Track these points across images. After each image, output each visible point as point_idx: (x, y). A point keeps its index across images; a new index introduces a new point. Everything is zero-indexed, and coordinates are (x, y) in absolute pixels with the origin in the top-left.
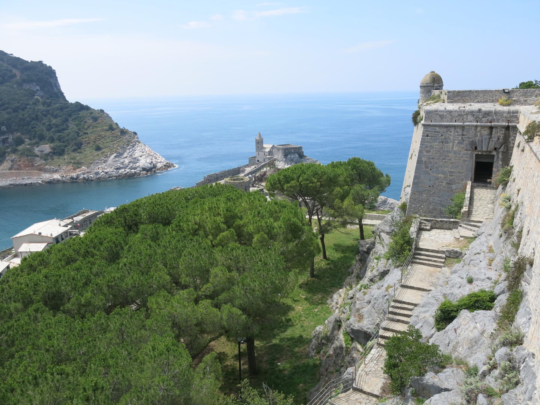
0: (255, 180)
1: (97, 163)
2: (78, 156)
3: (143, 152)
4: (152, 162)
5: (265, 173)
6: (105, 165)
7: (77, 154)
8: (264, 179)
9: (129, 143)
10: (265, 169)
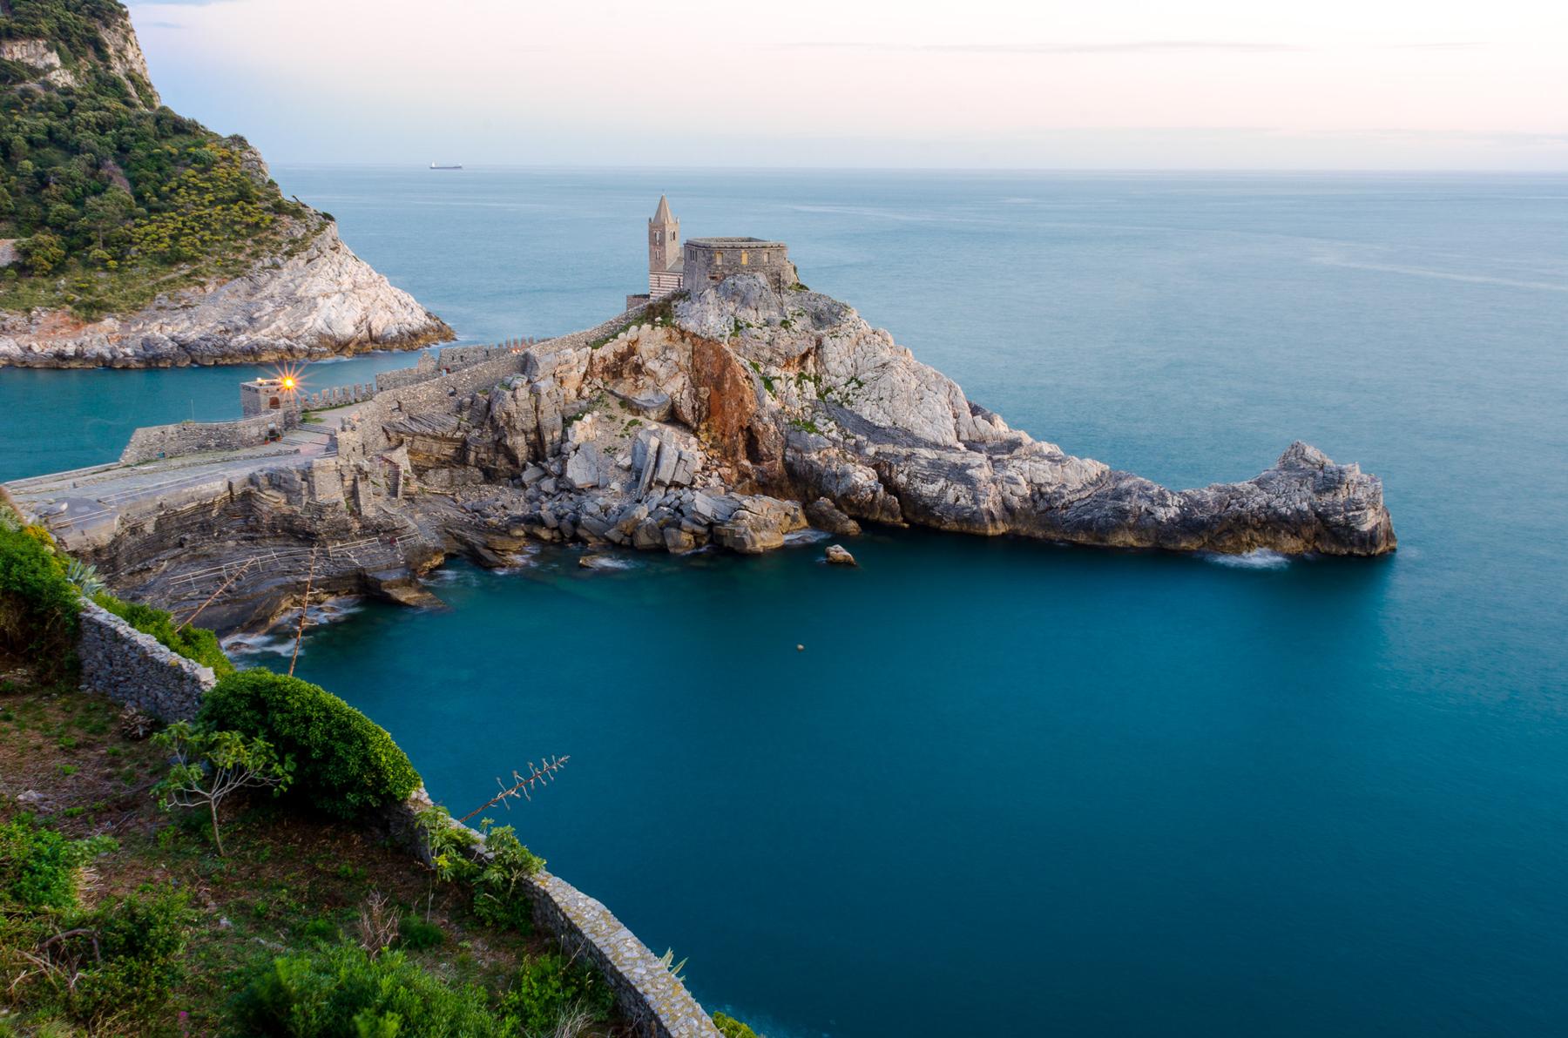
1: (160, 308)
2: (103, 282)
6: (184, 316)
7: (103, 275)
8: (626, 372)
9: (297, 246)
10: (634, 328)
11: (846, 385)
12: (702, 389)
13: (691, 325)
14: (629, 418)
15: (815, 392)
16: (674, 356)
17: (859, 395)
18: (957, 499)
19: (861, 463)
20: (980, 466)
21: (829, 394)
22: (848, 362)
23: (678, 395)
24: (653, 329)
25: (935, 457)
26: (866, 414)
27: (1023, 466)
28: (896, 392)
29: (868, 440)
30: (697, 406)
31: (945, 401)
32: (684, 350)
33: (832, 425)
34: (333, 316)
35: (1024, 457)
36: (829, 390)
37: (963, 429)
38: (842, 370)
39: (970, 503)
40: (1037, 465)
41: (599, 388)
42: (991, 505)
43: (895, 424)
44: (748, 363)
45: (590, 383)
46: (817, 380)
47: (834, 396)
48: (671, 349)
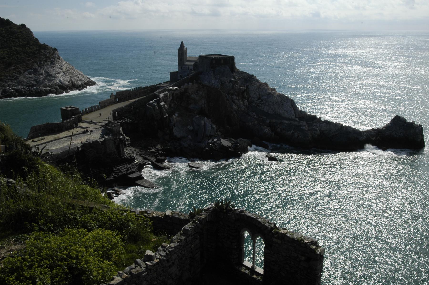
0: (173, 99)
3: (61, 69)
4: (71, 80)
5: (186, 90)
10: (186, 84)
11: (257, 101)
18: (298, 136)
20: (305, 126)
21: (252, 104)
23: (203, 106)
24: (193, 84)
25: (289, 123)
26: (265, 109)
34: (62, 79)
38: (255, 96)
40: (322, 125)
42: (309, 137)
46: (248, 99)
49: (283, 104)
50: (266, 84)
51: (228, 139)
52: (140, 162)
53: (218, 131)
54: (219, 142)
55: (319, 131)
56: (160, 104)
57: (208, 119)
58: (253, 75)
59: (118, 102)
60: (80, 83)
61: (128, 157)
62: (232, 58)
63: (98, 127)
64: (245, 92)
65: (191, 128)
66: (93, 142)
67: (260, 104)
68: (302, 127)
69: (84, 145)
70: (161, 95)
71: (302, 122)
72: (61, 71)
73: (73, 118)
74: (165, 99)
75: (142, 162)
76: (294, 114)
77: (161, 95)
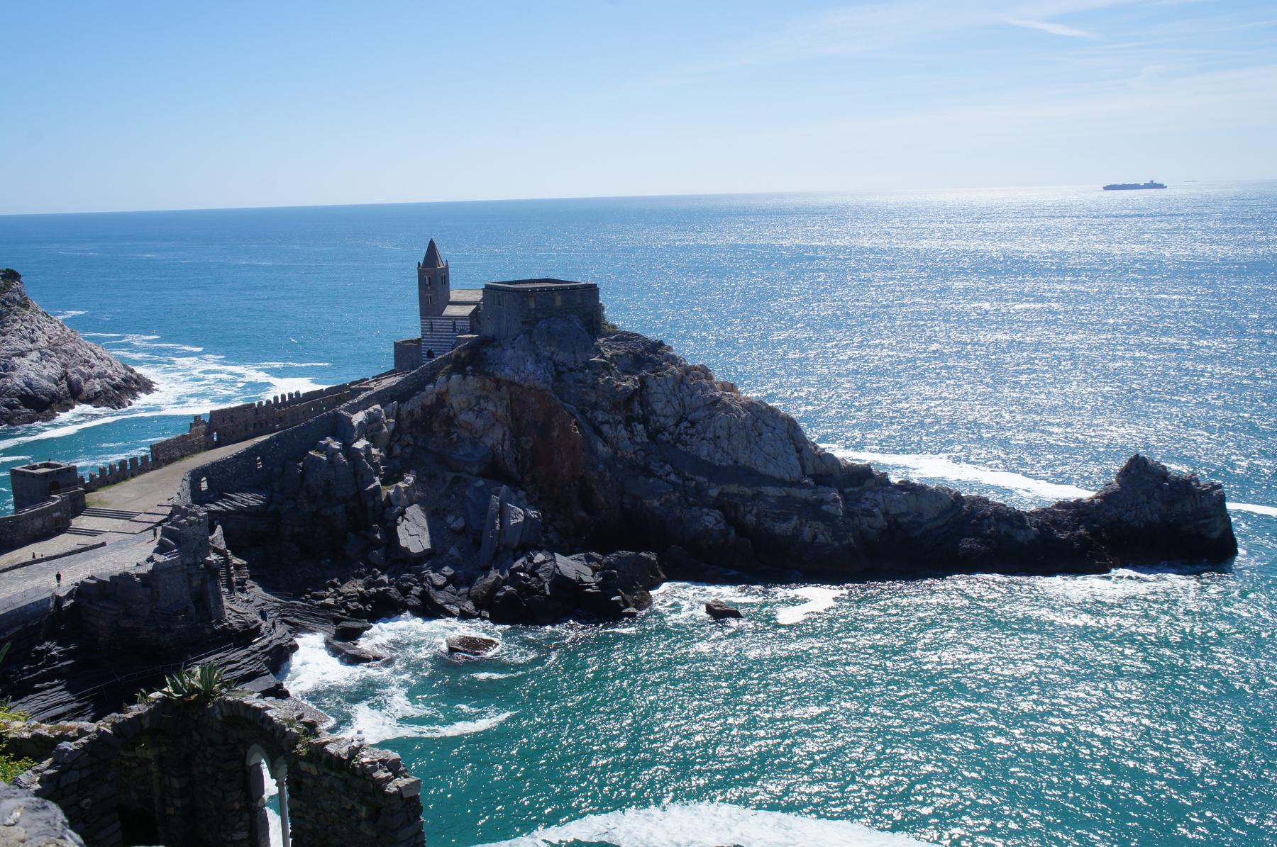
3: (33, 341)
4: (65, 376)
5: (441, 400)
8: (436, 426)
12: (524, 438)
13: (507, 373)
14: (450, 476)
15: (645, 434)
16: (491, 407)
17: (692, 435)
18: (815, 537)
19: (705, 505)
22: (676, 403)
24: (464, 378)
25: (784, 494)
26: (703, 454)
27: (876, 498)
28: (733, 430)
29: (709, 482)
30: (520, 457)
31: (784, 436)
32: (501, 399)
33: (668, 468)
34: (32, 375)
35: (876, 489)
36: (658, 431)
37: (809, 464)
38: (669, 411)
39: (830, 540)
41: (409, 445)
42: (852, 540)
43: (736, 462)
44: (575, 409)
45: (399, 440)
46: (645, 421)
47: (666, 437)
48: (486, 398)
49: (760, 435)
50: (705, 372)
51: (581, 555)
52: (279, 642)
53: (550, 528)
54: (552, 567)
55: (881, 517)
56: (354, 446)
57: (516, 492)
58: (661, 344)
59: (219, 444)
60: (97, 385)
61: (237, 626)
62: (592, 290)
63: (138, 527)
64: (638, 398)
65: (458, 524)
66: (112, 578)
67: (687, 434)
68: (824, 508)
69: (81, 591)
70: (358, 418)
71: (825, 489)
72: (31, 346)
73: (55, 499)
74: (371, 428)
75: (284, 641)
76: (797, 463)
77: (358, 418)
